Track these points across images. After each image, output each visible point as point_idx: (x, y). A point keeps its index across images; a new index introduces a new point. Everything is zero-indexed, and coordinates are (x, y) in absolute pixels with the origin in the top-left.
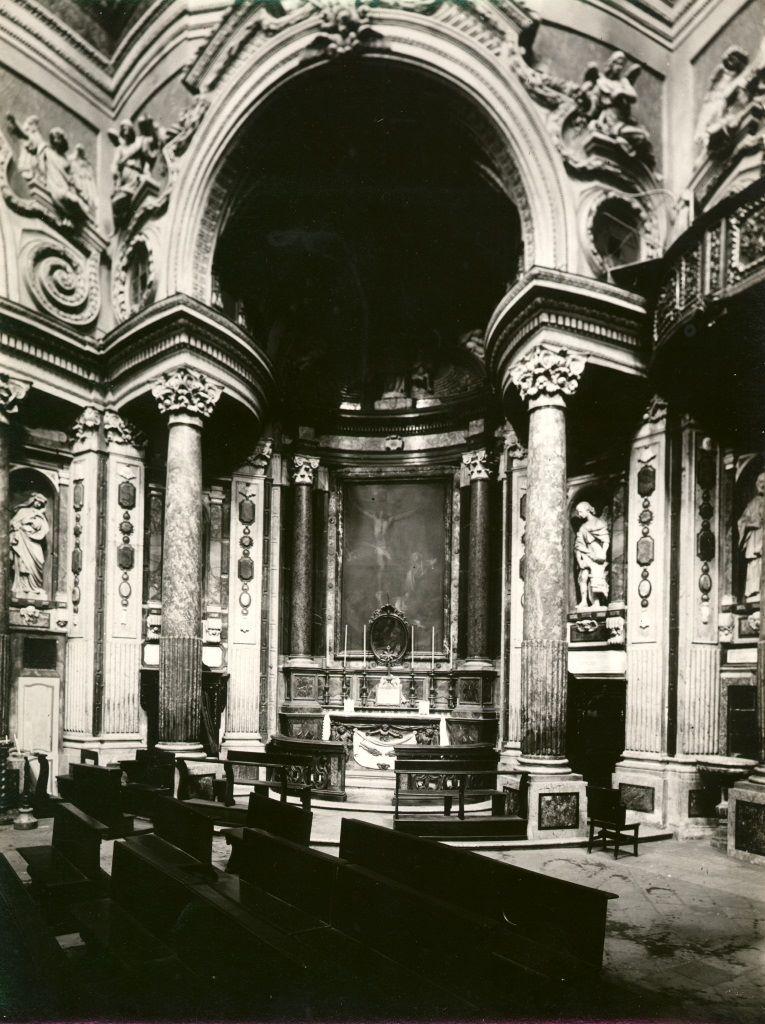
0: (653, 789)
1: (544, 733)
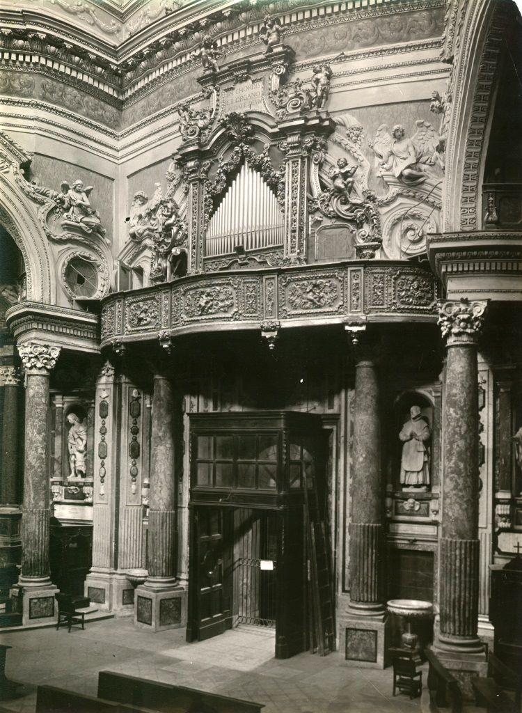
0: (104, 590)
1: (34, 563)
